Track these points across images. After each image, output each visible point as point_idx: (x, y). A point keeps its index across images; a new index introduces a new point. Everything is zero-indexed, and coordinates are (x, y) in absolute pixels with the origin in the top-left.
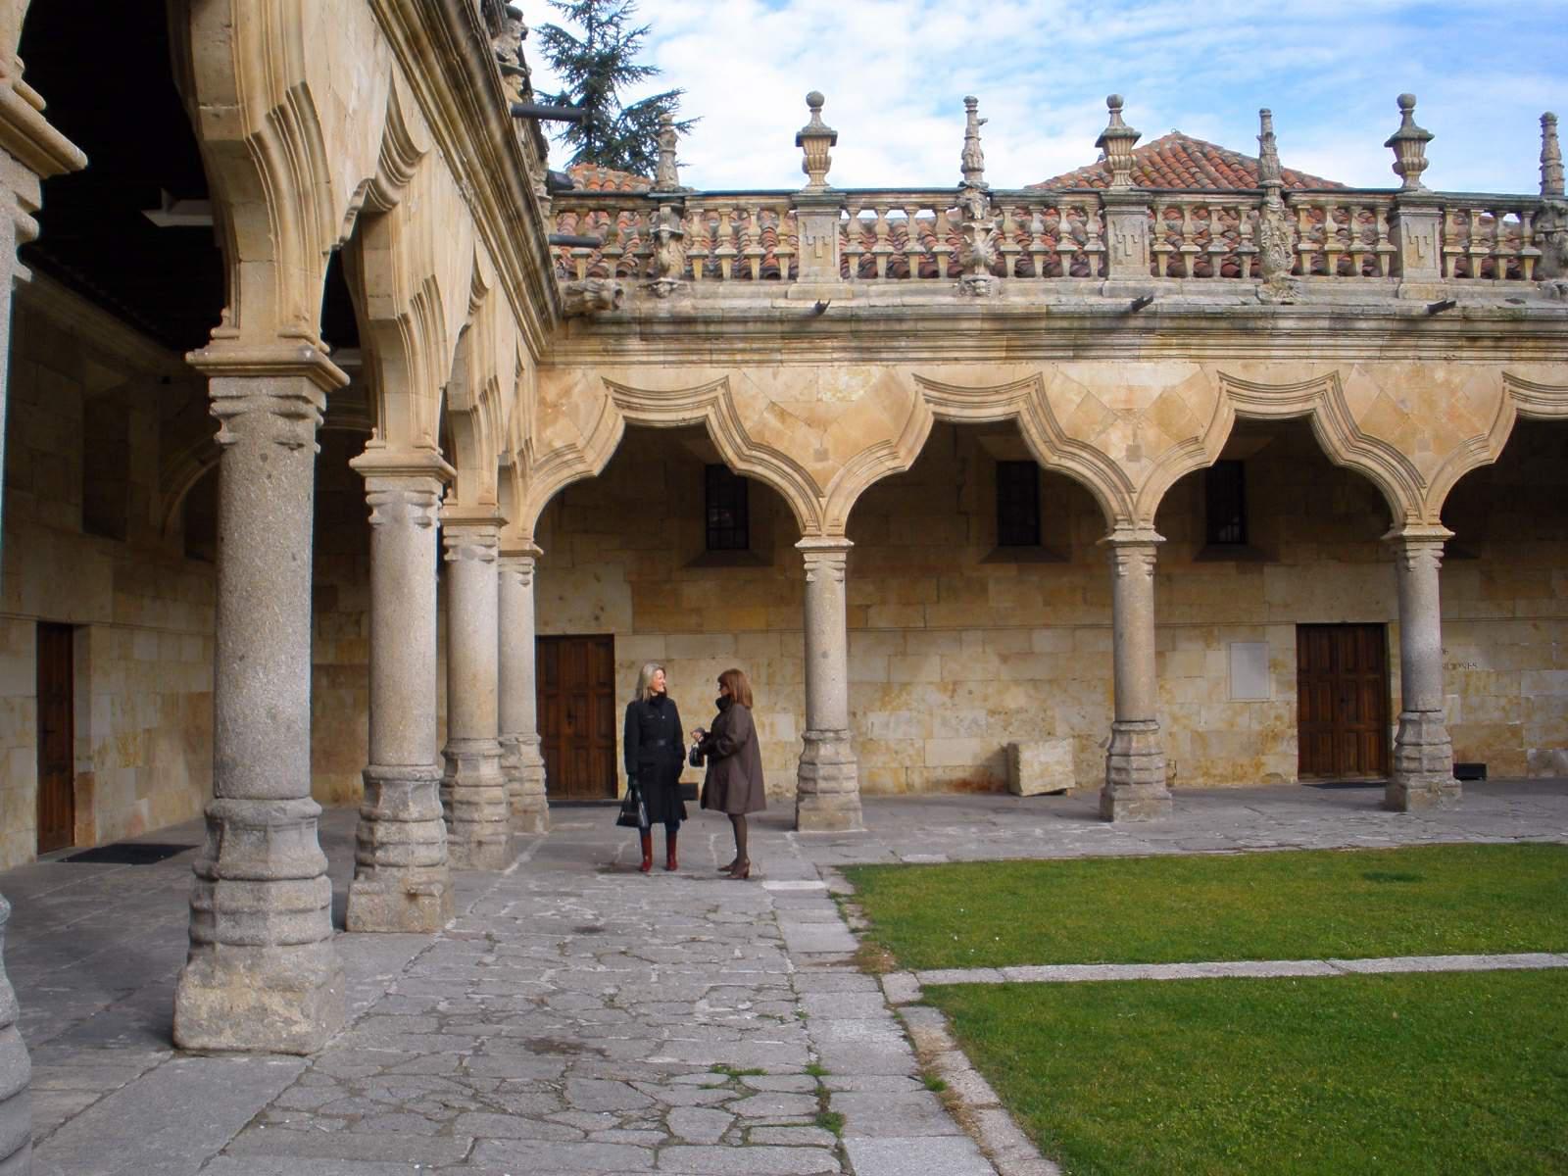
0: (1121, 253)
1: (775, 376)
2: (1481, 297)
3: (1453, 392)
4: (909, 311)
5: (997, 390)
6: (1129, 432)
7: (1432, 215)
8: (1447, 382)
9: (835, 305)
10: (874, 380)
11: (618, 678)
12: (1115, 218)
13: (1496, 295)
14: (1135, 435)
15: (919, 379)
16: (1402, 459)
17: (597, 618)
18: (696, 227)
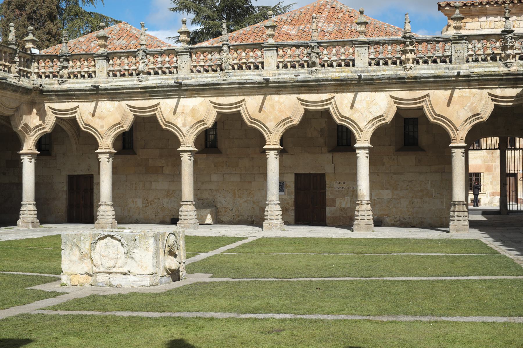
0: (181, 68)
1: (91, 105)
2: (288, 75)
3: (281, 104)
4: (120, 87)
5: (148, 108)
6: (183, 119)
7: (273, 50)
8: (279, 101)
9: (102, 86)
10: (116, 106)
11: (94, 187)
12: (180, 56)
13: (292, 74)
14: (185, 120)
15: (128, 106)
16: (265, 125)
17: (89, 170)
18: (71, 63)
